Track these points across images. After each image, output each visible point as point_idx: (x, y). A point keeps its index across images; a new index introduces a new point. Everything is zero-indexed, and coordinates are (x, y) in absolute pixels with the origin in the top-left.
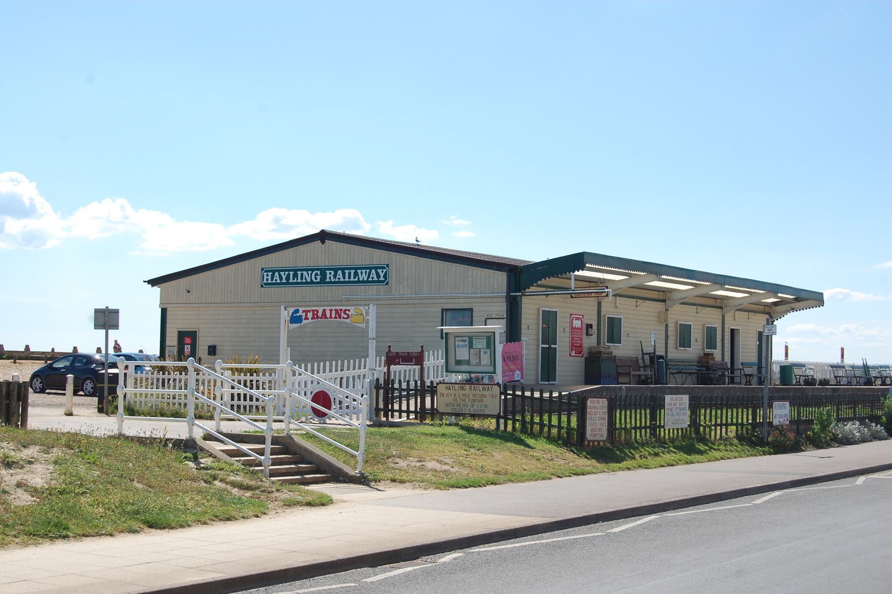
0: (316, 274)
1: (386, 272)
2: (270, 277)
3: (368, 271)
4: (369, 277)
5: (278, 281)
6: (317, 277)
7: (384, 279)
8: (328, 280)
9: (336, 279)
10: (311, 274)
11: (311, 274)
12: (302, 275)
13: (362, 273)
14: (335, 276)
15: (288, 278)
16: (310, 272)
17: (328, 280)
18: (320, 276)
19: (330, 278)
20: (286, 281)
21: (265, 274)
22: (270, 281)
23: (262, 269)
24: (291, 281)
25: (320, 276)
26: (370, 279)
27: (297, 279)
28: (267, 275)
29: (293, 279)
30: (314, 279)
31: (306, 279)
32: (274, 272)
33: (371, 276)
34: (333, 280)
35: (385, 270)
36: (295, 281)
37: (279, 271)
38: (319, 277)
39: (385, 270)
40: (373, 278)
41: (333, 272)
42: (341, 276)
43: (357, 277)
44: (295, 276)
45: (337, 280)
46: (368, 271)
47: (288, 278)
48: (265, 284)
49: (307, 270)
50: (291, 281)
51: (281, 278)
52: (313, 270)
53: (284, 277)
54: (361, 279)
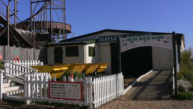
2: (103, 39)
15: (110, 39)
21: (101, 38)
22: (103, 40)
24: (112, 40)
37: (107, 37)
44: (113, 38)
47: (110, 39)
48: (101, 42)
50: (112, 40)
51: (108, 39)
53: (109, 39)
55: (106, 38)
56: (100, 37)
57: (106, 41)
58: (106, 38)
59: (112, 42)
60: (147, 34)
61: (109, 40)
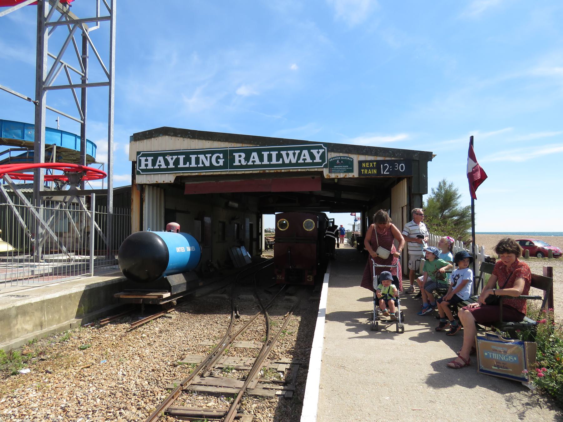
0: (218, 158)
1: (324, 153)
2: (150, 163)
3: (297, 152)
4: (299, 158)
5: (164, 166)
6: (219, 160)
7: (321, 161)
8: (237, 163)
9: (248, 162)
10: (211, 158)
11: (211, 158)
12: (197, 160)
13: (288, 155)
14: (247, 159)
15: (177, 162)
16: (208, 156)
18: (224, 160)
19: (240, 161)
20: (174, 167)
21: (143, 159)
22: (150, 167)
23: (138, 153)
25: (224, 160)
26: (301, 161)
27: (190, 164)
28: (146, 160)
29: (185, 163)
31: (203, 163)
33: (302, 157)
34: (244, 163)
35: (321, 151)
36: (187, 165)
37: (164, 155)
39: (321, 151)
40: (305, 159)
41: (243, 155)
43: (281, 159)
44: (187, 160)
45: (250, 163)
46: (297, 152)
47: (177, 162)
48: (143, 170)
49: (204, 153)
50: (181, 165)
51: (167, 163)
52: (213, 153)
54: (287, 161)
55: (161, 158)
56: (138, 153)
57: (160, 170)
58: (161, 158)
59: (181, 173)
60: (309, 149)
61: (171, 166)
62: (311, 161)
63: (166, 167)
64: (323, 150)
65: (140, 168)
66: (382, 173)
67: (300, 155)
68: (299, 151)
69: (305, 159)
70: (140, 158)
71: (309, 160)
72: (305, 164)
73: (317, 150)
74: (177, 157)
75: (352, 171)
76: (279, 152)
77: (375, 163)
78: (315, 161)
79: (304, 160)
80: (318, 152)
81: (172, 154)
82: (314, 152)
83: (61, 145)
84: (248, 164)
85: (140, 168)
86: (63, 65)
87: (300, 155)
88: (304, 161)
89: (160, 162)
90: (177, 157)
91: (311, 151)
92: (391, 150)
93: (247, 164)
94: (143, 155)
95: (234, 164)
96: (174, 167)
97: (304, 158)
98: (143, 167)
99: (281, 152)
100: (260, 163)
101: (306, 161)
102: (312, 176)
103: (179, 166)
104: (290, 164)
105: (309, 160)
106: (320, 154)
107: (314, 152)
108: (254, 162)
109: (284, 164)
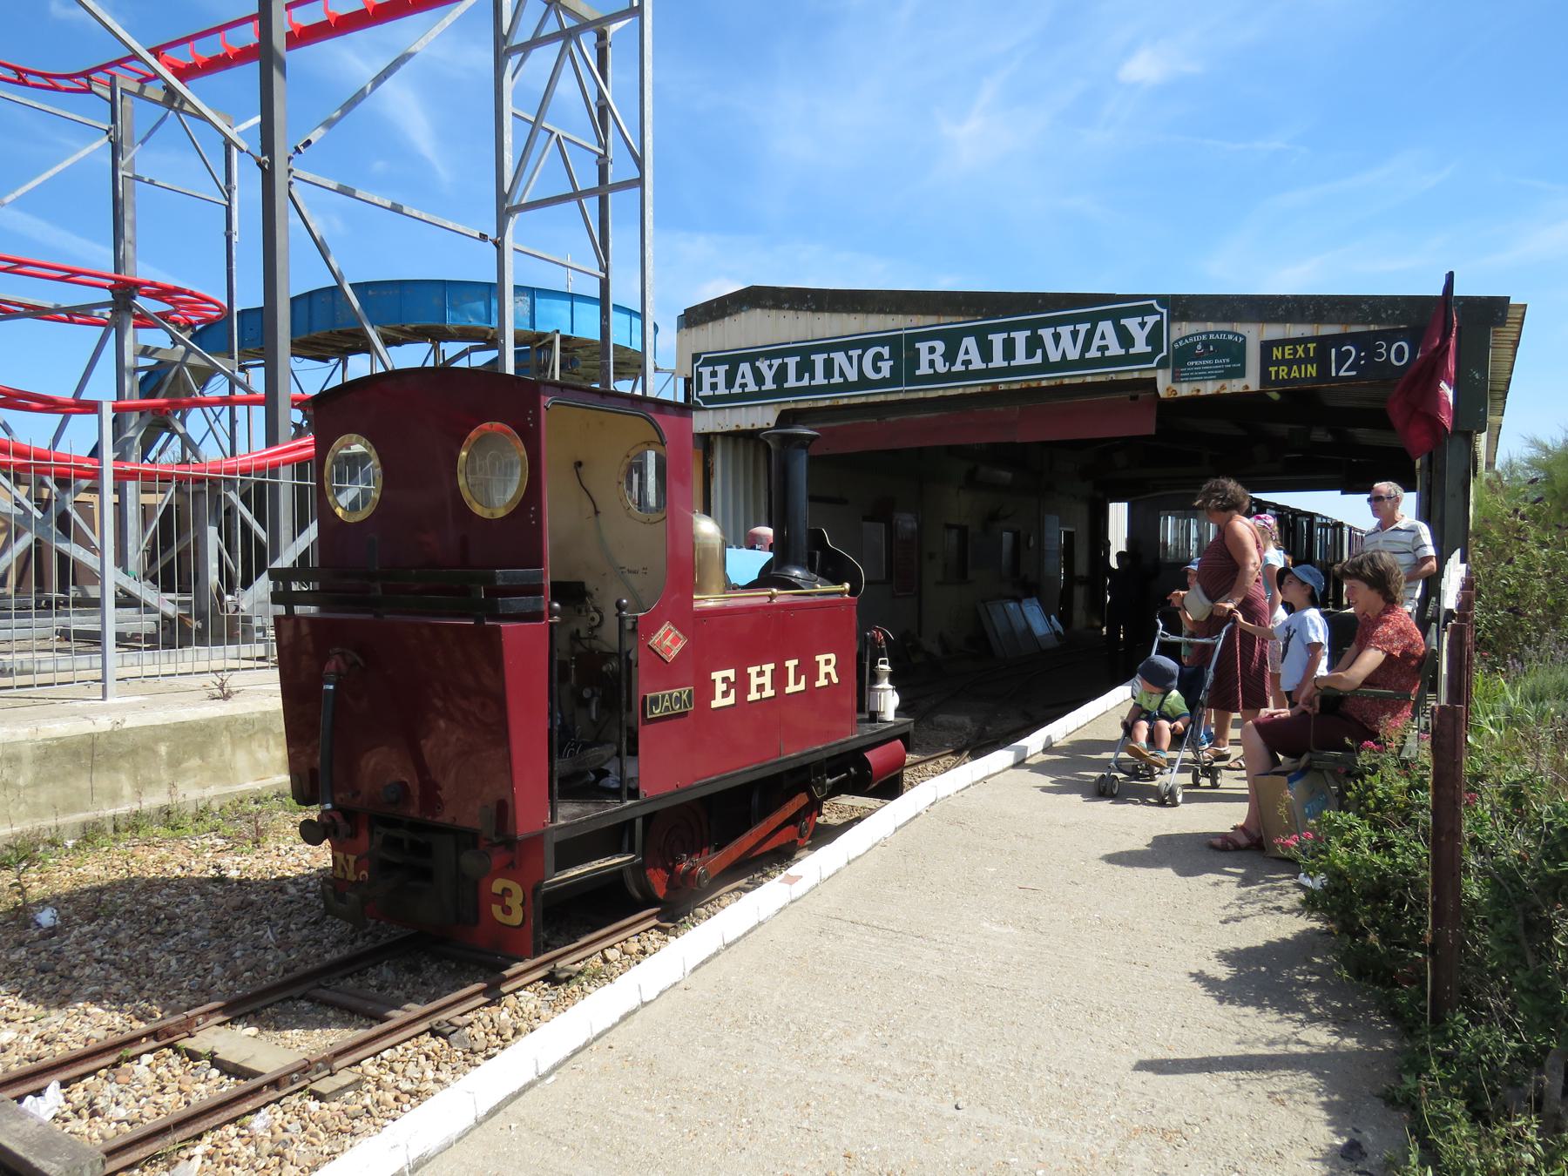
0: (878, 357)
1: (1158, 325)
2: (721, 380)
3: (1083, 328)
4: (1087, 346)
5: (752, 387)
6: (879, 364)
7: (1149, 349)
8: (924, 369)
9: (953, 363)
10: (860, 358)
11: (860, 358)
12: (829, 365)
13: (1057, 338)
14: (950, 357)
15: (781, 375)
16: (855, 353)
17: (924, 369)
18: (891, 363)
19: (932, 363)
20: (774, 387)
21: (706, 371)
22: (722, 390)
23: (696, 357)
24: (791, 382)
25: (891, 363)
26: (1093, 353)
27: (812, 377)
28: (714, 374)
29: (799, 378)
30: (870, 373)
31: (842, 374)
32: (733, 361)
33: (1096, 342)
34: (941, 368)
35: (1151, 320)
36: (805, 382)
37: (752, 358)
38: (886, 367)
39: (1151, 320)
40: (1106, 348)
41: (940, 346)
42: (975, 355)
43: (1039, 352)
44: (805, 367)
45: (958, 367)
46: (1083, 328)
47: (781, 375)
48: (707, 400)
49: (845, 347)
50: (791, 382)
51: (759, 378)
52: (865, 345)
53: (769, 375)
54: (1054, 357)
55: (745, 367)
56: (696, 357)
57: (744, 396)
59: (791, 403)
60: (1115, 317)
61: (769, 385)
62: (1122, 352)
63: (757, 389)
64: (1157, 318)
65: (700, 394)
66: (1334, 374)
67: (1090, 335)
68: (1088, 326)
69: (1106, 348)
70: (700, 369)
71: (1115, 350)
72: (1104, 361)
73: (1140, 320)
74: (780, 361)
75: (1240, 373)
76: (1034, 332)
77: (1312, 346)
78: (1132, 351)
79: (1103, 349)
80: (1143, 325)
81: (770, 355)
82: (1131, 324)
83: (572, 332)
84: (954, 369)
85: (700, 394)
86: (555, 136)
87: (1090, 335)
88: (1103, 354)
89: (743, 377)
90: (780, 361)
91: (1123, 322)
92: (1366, 303)
93: (950, 369)
94: (707, 362)
95: (918, 373)
96: (774, 387)
97: (1103, 343)
98: (707, 391)
99: (1040, 332)
100: (984, 366)
101: (1107, 353)
102: (1130, 393)
103: (786, 385)
104: (1064, 364)
105: (1115, 350)
106: (1148, 328)
107: (1131, 324)
108: (967, 363)
109: (1047, 366)
